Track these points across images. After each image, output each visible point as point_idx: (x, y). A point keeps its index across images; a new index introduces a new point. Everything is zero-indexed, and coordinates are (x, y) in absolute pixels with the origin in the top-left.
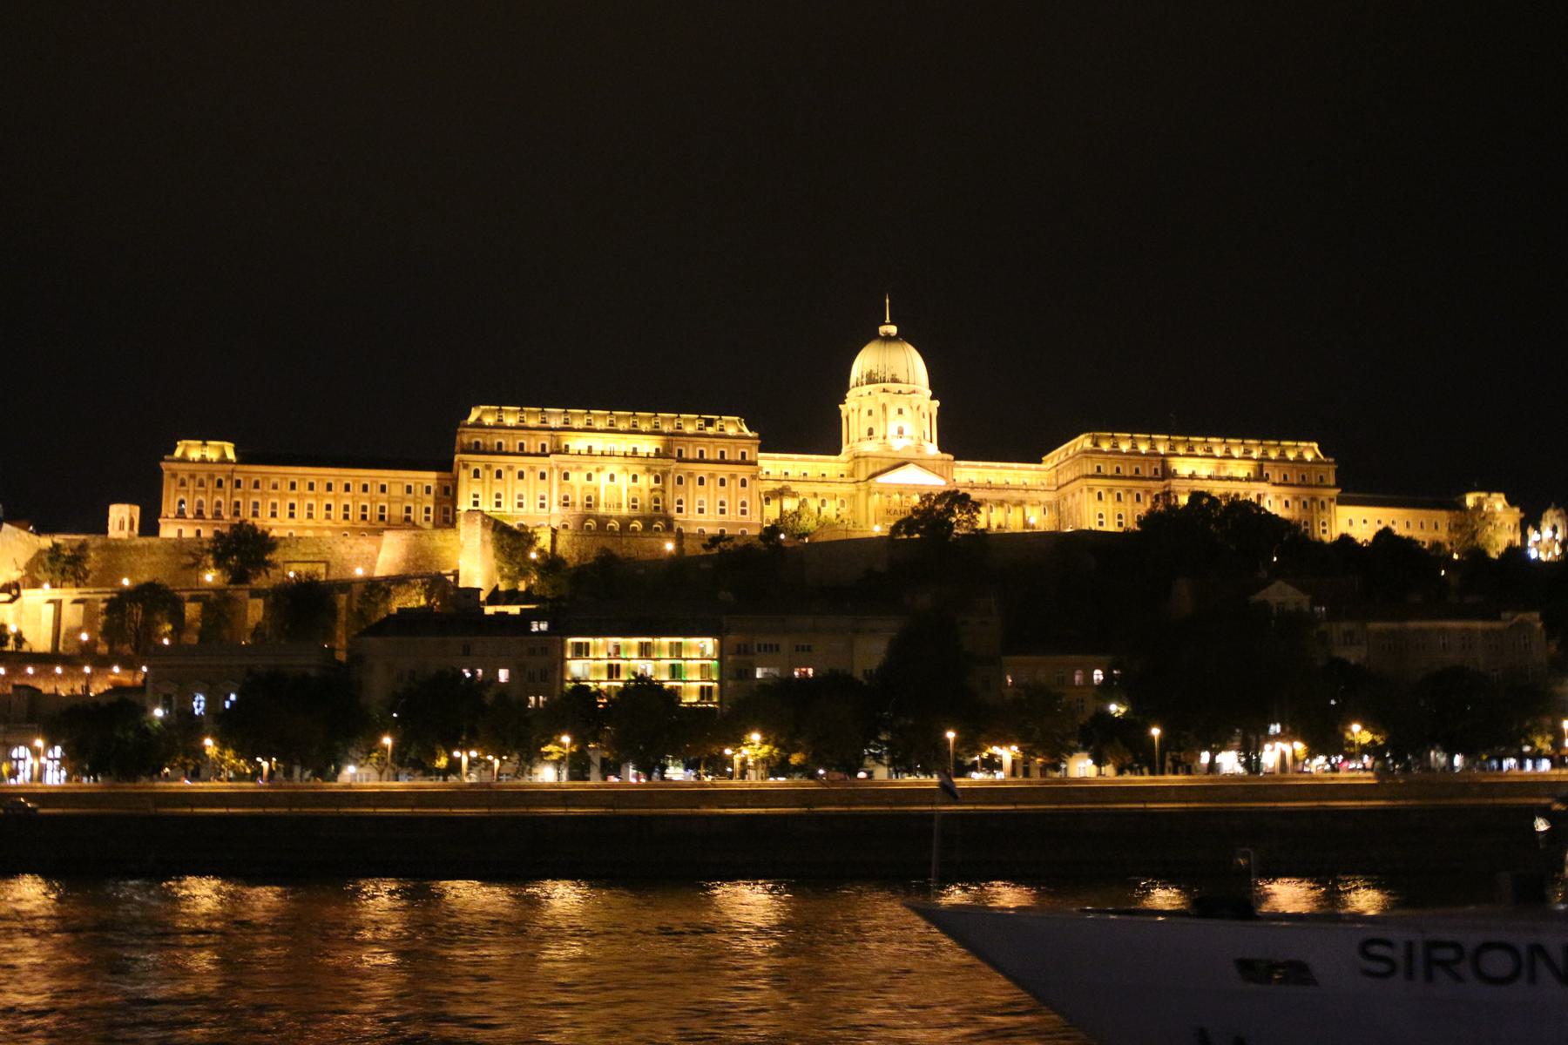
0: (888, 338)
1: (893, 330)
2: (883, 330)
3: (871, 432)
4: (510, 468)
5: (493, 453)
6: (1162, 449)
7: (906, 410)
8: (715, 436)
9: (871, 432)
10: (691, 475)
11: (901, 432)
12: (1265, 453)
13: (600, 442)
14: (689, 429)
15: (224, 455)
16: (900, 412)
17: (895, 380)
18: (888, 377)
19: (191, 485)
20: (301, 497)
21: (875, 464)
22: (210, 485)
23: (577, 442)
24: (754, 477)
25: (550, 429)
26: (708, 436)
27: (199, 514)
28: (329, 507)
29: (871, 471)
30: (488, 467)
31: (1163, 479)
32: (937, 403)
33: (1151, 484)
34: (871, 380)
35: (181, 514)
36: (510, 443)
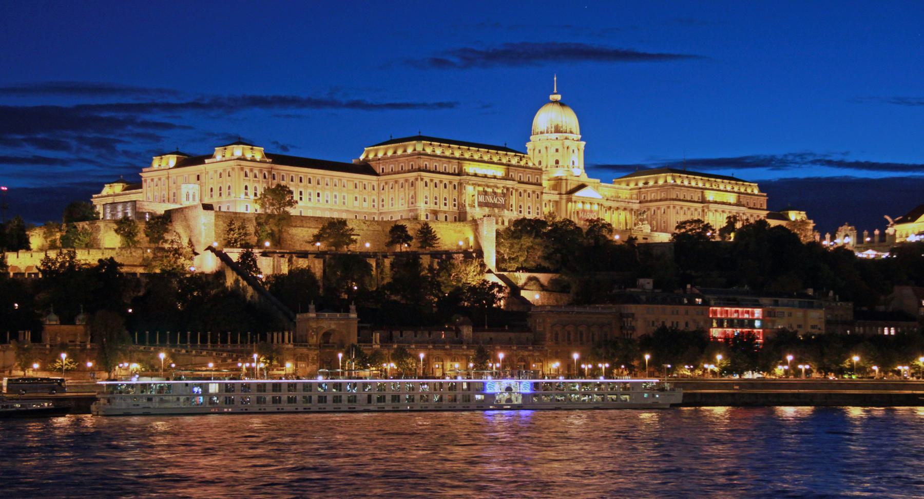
0: (562, 104)
1: (558, 97)
2: (552, 97)
3: (557, 162)
5: (433, 172)
6: (700, 185)
7: (576, 151)
9: (557, 162)
13: (481, 169)
14: (514, 161)
17: (571, 132)
19: (250, 175)
20: (306, 187)
22: (260, 177)
23: (470, 168)
25: (458, 159)
28: (318, 195)
29: (569, 188)
31: (702, 202)
32: (583, 143)
34: (558, 130)
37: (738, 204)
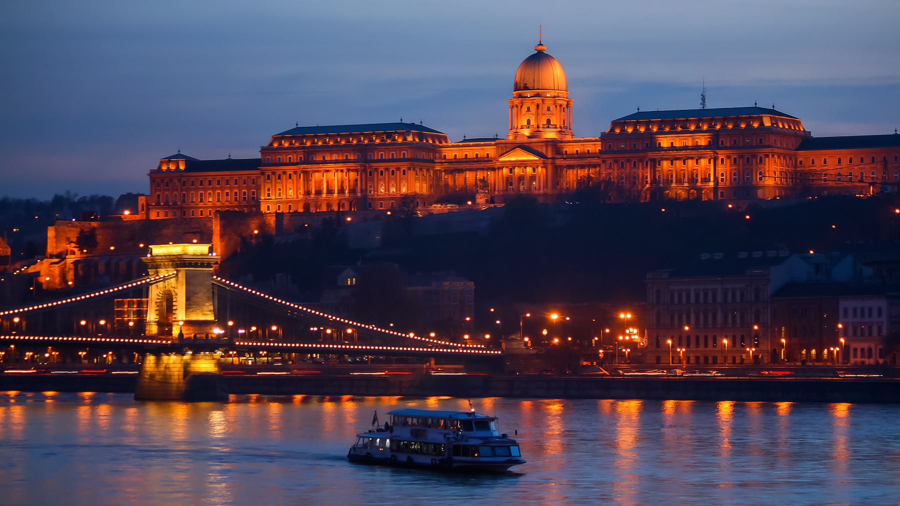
4: (284, 173)
8: (389, 145)
10: (376, 170)
11: (529, 122)
12: (723, 126)
15: (178, 167)
16: (529, 109)
17: (526, 88)
18: (522, 86)
21: (502, 149)
24: (409, 169)
26: (385, 145)
27: (166, 203)
30: (274, 173)
33: (642, 154)
35: (158, 204)
36: (285, 158)
37: (714, 145)
